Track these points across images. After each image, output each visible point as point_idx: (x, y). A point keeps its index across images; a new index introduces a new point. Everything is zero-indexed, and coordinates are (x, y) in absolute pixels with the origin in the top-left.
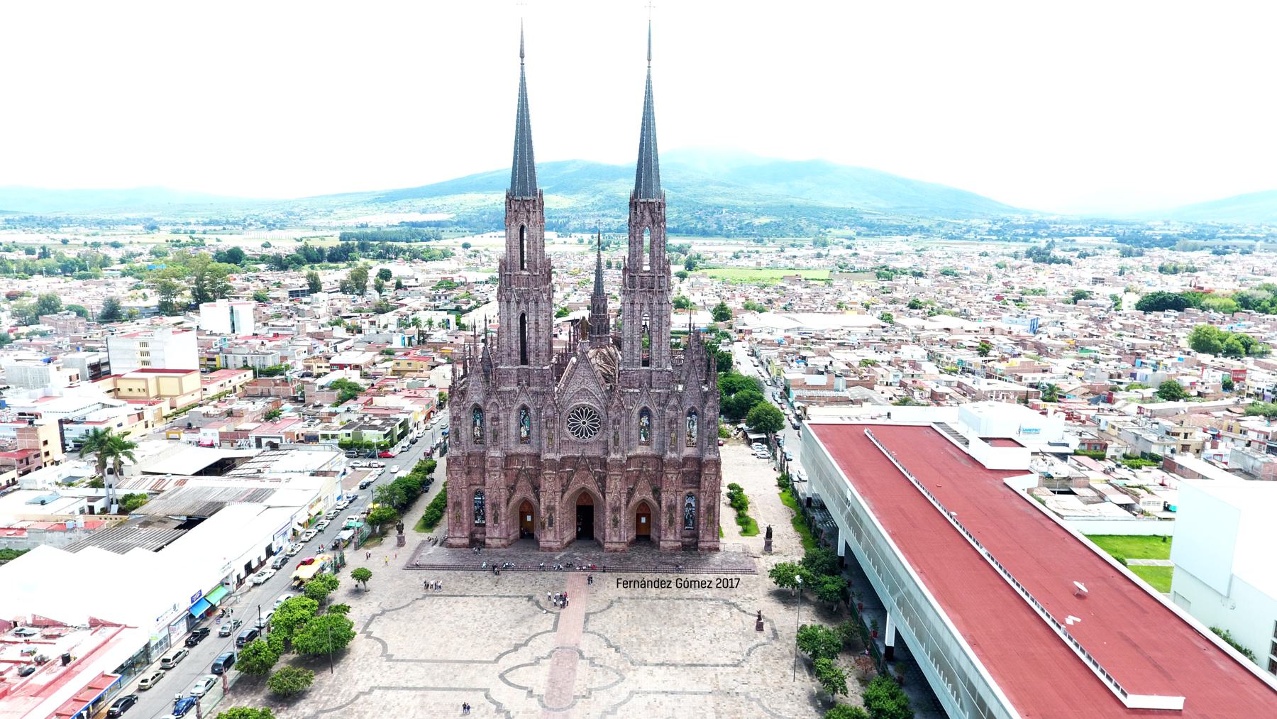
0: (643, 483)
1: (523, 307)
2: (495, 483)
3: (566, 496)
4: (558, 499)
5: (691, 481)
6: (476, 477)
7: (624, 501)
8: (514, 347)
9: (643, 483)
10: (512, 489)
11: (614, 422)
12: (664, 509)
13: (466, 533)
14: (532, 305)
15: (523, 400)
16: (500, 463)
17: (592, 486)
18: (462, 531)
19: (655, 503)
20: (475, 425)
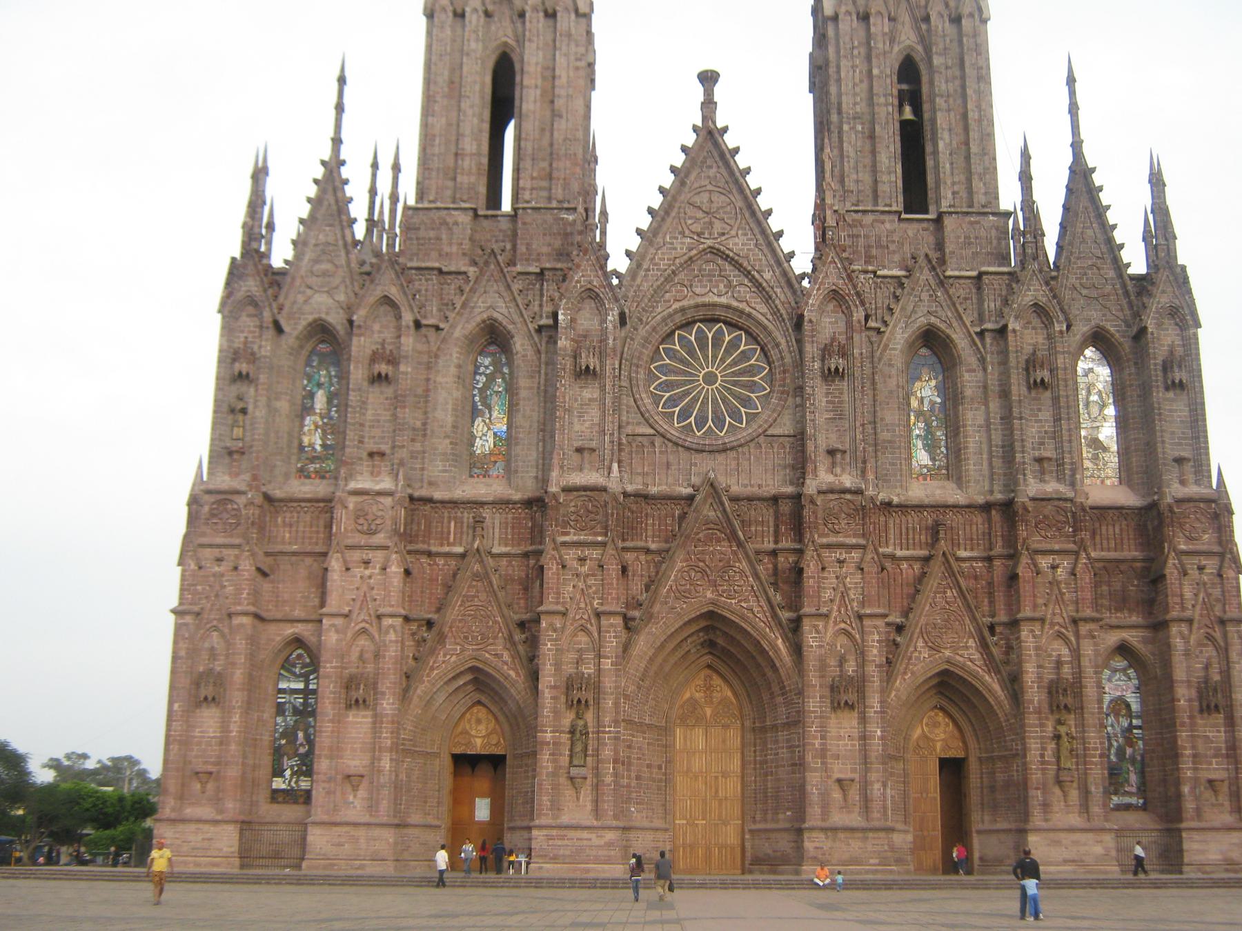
0: (937, 600)
1: (503, 32)
2: (366, 588)
3: (643, 644)
4: (612, 643)
5: (1121, 602)
6: (292, 589)
7: (875, 652)
8: (469, 146)
9: (937, 600)
10: (427, 629)
11: (826, 352)
12: (1034, 695)
13: (231, 806)
14: (536, 22)
15: (492, 303)
16: (389, 512)
17: (750, 606)
18: (217, 800)
19: (993, 685)
20: (307, 410)
